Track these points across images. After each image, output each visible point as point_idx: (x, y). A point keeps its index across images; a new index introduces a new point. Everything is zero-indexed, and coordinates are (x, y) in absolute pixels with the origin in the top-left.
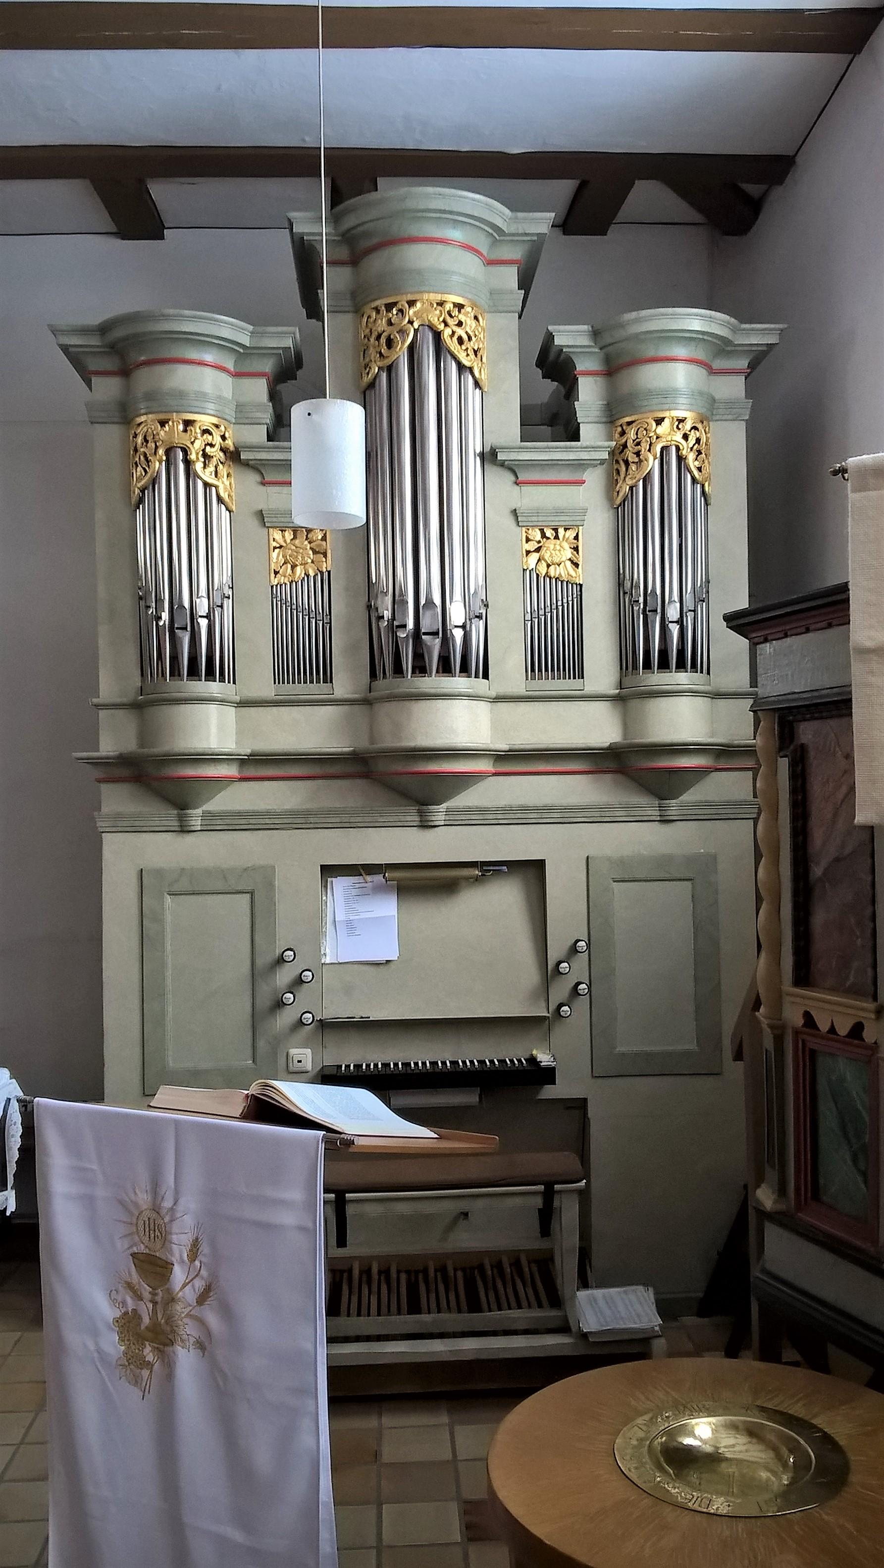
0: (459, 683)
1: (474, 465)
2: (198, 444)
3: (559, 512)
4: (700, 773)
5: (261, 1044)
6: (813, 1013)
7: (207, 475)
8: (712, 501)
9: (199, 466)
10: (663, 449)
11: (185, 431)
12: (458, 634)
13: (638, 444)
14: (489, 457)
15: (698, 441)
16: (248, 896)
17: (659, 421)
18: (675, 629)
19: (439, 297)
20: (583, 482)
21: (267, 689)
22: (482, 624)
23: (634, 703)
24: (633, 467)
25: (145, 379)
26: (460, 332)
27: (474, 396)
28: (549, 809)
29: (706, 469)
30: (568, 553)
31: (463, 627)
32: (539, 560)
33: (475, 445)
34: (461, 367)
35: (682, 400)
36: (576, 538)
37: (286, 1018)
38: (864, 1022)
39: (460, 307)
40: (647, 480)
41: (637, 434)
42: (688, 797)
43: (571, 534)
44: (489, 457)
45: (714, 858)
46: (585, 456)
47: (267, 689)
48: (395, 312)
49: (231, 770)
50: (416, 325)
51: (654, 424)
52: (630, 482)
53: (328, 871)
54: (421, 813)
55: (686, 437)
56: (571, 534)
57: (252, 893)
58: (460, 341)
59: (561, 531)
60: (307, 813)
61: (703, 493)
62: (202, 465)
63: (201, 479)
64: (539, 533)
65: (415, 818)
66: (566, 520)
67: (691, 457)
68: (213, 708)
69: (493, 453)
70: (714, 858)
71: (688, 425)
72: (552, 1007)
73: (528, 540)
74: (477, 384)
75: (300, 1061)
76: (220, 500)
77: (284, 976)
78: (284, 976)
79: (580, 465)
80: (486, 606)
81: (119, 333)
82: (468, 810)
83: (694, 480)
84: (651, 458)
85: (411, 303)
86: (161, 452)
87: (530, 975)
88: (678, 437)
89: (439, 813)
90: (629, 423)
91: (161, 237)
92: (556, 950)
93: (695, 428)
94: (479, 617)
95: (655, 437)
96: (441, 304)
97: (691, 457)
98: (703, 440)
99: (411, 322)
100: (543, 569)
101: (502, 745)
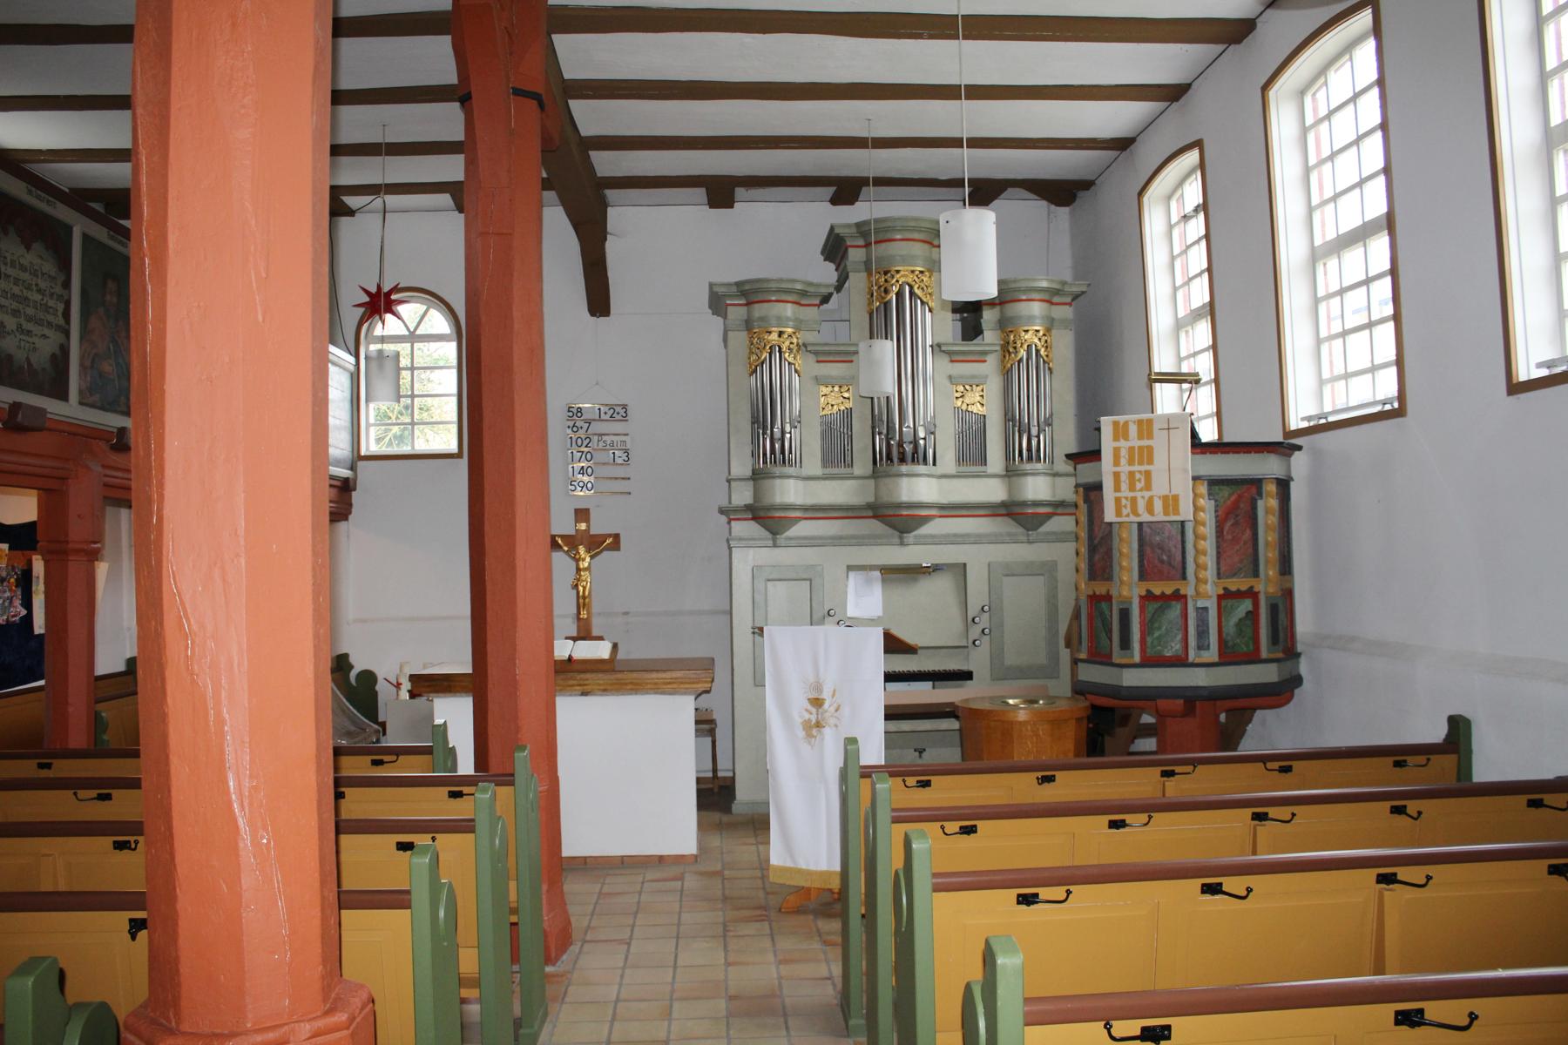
0: (921, 469)
1: (929, 350)
2: (787, 343)
3: (973, 377)
4: (1049, 516)
7: (791, 360)
8: (1054, 371)
10: (1028, 346)
12: (922, 442)
14: (937, 348)
15: (1046, 341)
16: (808, 582)
17: (1027, 331)
19: (912, 268)
20: (985, 361)
21: (819, 471)
22: (933, 436)
23: (1014, 479)
24: (1013, 355)
25: (759, 310)
26: (922, 285)
27: (928, 315)
28: (968, 535)
29: (1050, 356)
30: (979, 399)
31: (925, 439)
33: (929, 342)
34: (922, 302)
35: (1038, 321)
36: (983, 390)
39: (921, 272)
42: (1043, 529)
44: (937, 348)
46: (987, 348)
47: (819, 471)
48: (889, 275)
49: (798, 514)
50: (900, 283)
52: (1011, 362)
53: (850, 568)
54: (901, 538)
55: (1040, 339)
56: (979, 388)
57: (811, 580)
59: (974, 386)
60: (841, 538)
61: (1049, 369)
65: (897, 540)
66: (977, 381)
68: (792, 481)
69: (939, 345)
71: (1041, 333)
72: (971, 641)
74: (930, 310)
76: (796, 371)
79: (985, 353)
80: (935, 426)
81: (747, 287)
82: (925, 536)
83: (1044, 360)
85: (898, 272)
87: (958, 625)
88: (1036, 340)
89: (910, 537)
90: (1012, 331)
91: (732, 207)
92: (973, 610)
93: (1044, 335)
94: (932, 433)
96: (913, 272)
97: (1043, 350)
98: (1049, 341)
99: (897, 281)
100: (965, 405)
101: (944, 501)
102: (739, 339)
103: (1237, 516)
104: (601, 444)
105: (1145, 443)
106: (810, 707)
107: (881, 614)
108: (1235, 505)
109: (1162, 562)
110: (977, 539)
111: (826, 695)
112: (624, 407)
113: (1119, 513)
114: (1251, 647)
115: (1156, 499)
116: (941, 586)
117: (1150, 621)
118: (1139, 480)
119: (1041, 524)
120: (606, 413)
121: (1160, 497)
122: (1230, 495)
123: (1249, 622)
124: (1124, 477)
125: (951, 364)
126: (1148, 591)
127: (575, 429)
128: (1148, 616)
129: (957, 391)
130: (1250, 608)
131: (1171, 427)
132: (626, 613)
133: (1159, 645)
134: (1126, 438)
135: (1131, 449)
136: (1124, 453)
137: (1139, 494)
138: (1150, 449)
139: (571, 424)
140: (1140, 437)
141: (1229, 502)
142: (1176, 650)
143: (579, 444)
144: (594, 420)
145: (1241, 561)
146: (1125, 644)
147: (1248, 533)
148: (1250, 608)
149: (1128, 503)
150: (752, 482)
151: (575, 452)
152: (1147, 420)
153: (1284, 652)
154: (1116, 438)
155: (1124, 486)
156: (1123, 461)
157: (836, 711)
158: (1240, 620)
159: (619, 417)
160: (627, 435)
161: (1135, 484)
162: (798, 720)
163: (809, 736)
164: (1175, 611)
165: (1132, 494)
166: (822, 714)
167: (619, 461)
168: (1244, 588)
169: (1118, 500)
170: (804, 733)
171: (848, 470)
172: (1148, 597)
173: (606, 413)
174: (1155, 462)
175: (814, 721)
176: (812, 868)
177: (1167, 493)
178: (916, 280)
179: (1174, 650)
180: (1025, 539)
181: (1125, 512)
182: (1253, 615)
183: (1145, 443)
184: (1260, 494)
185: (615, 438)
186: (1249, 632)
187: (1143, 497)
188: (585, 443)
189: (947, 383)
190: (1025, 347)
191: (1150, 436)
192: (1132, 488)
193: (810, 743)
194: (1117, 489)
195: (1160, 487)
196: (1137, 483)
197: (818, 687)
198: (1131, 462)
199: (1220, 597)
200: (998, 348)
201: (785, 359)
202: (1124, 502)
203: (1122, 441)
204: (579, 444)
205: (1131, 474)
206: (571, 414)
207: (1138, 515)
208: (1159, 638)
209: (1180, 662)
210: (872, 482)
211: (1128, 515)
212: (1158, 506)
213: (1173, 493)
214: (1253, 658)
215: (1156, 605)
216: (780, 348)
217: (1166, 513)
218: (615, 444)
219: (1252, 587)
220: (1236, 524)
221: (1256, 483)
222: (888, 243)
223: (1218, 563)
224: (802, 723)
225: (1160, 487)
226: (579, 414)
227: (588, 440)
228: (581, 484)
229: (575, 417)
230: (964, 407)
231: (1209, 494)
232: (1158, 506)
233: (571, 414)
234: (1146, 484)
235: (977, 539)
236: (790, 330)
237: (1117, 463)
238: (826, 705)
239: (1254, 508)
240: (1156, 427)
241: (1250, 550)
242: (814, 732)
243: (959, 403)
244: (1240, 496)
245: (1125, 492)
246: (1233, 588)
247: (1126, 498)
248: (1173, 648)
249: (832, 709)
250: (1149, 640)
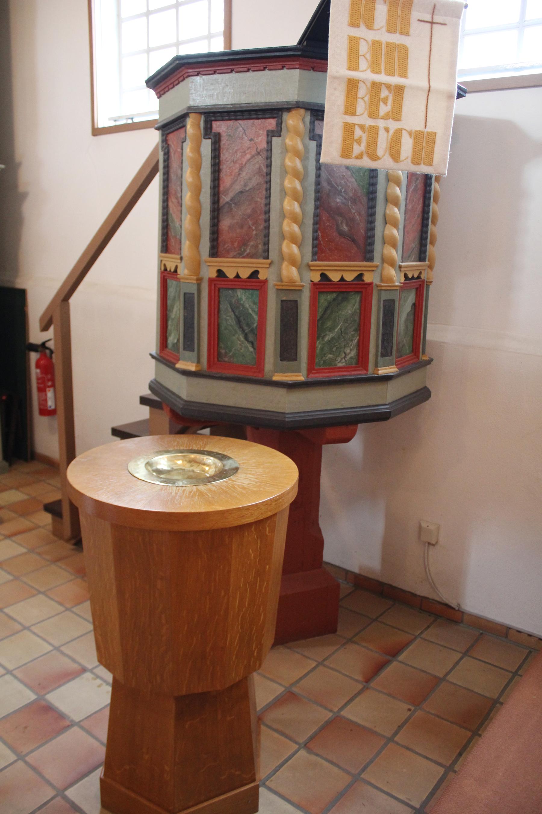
6: (224, 270)
38: (259, 269)
105: (396, 39)
109: (341, 234)
113: (346, 152)
115: (405, 135)
118: (385, 102)
121: (410, 134)
128: (320, 311)
131: (435, 21)
136: (364, 48)
137: (381, 124)
138: (404, 51)
142: (351, 358)
154: (354, 24)
155: (361, 107)
156: (363, 64)
161: (378, 107)
165: (369, 122)
169: (348, 129)
174: (410, 74)
177: (421, 128)
179: (348, 357)
181: (357, 149)
183: (396, 39)
187: (387, 130)
191: (405, 32)
194: (350, 110)
202: (358, 132)
203: (362, 26)
205: (376, 87)
208: (329, 341)
211: (359, 157)
213: (429, 129)
237: (353, 65)
247: (362, 127)
250: (319, 345)
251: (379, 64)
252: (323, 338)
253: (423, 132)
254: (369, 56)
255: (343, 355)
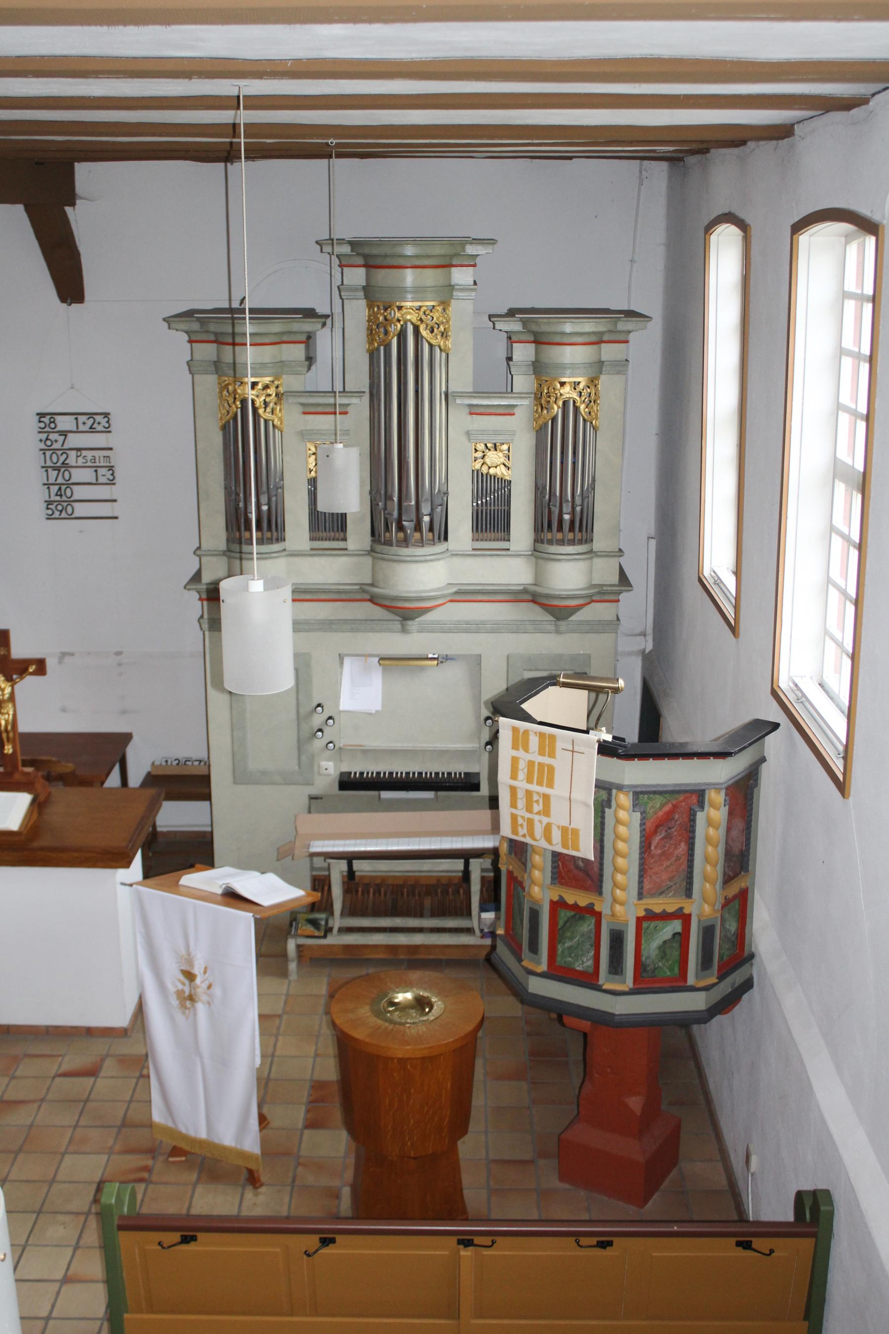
3: (496, 433)
4: (579, 608)
5: (303, 757)
9: (261, 411)
11: (253, 388)
13: (549, 397)
17: (563, 384)
18: (567, 517)
20: (513, 414)
24: (545, 412)
28: (483, 623)
30: (502, 460)
31: (429, 515)
32: (483, 464)
37: (319, 743)
40: (554, 420)
41: (548, 389)
42: (574, 618)
43: (505, 447)
45: (589, 657)
51: (558, 386)
54: (403, 625)
56: (505, 447)
58: (432, 331)
62: (263, 410)
63: (262, 417)
64: (483, 446)
67: (582, 407)
70: (589, 657)
73: (476, 450)
75: (326, 769)
77: (318, 719)
78: (318, 719)
82: (432, 622)
83: (584, 420)
84: (555, 407)
86: (238, 403)
88: (575, 395)
89: (413, 625)
95: (559, 394)
98: (593, 395)
102: (209, 382)
103: (670, 828)
104: (81, 460)
105: (546, 760)
106: (182, 978)
107: (379, 708)
108: (669, 816)
110: (496, 628)
111: (197, 970)
112: (106, 415)
114: (676, 970)
116: (454, 673)
117: (562, 927)
119: (571, 614)
120: (84, 423)
121: (558, 827)
122: (662, 806)
123: (676, 945)
124: (520, 794)
125: (469, 417)
126: (561, 897)
127: (49, 443)
129: (476, 450)
130: (679, 929)
132: (119, 653)
133: (570, 956)
134: (526, 749)
135: (531, 764)
136: (522, 765)
137: (536, 818)
138: (551, 769)
139: (44, 436)
140: (541, 752)
141: (661, 813)
142: (588, 966)
143: (55, 460)
144: (71, 432)
145: (671, 879)
146: (534, 947)
147: (683, 847)
148: (679, 929)
149: (525, 824)
150: (225, 559)
151: (50, 470)
152: (549, 735)
153: (717, 978)
154: (515, 747)
155: (521, 803)
156: (521, 775)
157: (209, 987)
158: (665, 942)
159: (99, 428)
160: (111, 449)
161: (532, 806)
162: (172, 989)
163: (183, 1006)
164: (587, 926)
165: (528, 815)
166: (194, 989)
167: (102, 480)
168: (671, 909)
169: (514, 818)
170: (178, 1002)
171: (341, 544)
172: (557, 905)
173: (84, 423)
174: (555, 786)
175: (187, 993)
176: (192, 1133)
177: (566, 824)
178: (423, 317)
179: (585, 965)
180: (551, 628)
182: (683, 937)
183: (546, 760)
184: (702, 807)
185: (97, 453)
186: (676, 954)
187: (540, 821)
188: (62, 458)
189: (464, 439)
190: (560, 403)
191: (552, 755)
192: (529, 809)
193: (184, 1013)
194: (514, 805)
195: (559, 816)
196: (535, 805)
197: (190, 961)
198: (529, 780)
199: (639, 920)
200: (533, 396)
201: (259, 416)
202: (520, 821)
204: (55, 460)
206: (42, 425)
207: (535, 840)
208: (570, 948)
209: (589, 980)
210: (368, 560)
211: (524, 836)
212: (556, 835)
213: (572, 826)
214: (678, 984)
215: (570, 913)
216: (253, 401)
217: (565, 845)
218: (97, 460)
219: (681, 909)
220: (668, 837)
221: (699, 795)
222: (387, 270)
223: (641, 883)
224: (175, 992)
225: (559, 816)
226: (52, 425)
227: (64, 456)
228: (60, 508)
229: (47, 429)
230: (485, 470)
231: (634, 806)
232: (556, 835)
233: (42, 425)
234: (544, 804)
235: (496, 628)
236: (267, 380)
237: (514, 776)
238: (198, 981)
239: (692, 820)
240: (559, 745)
241: (684, 866)
242: (188, 1003)
243: (477, 466)
244: (675, 807)
245: (521, 812)
246: (658, 910)
247: (523, 817)
248: (584, 964)
249: (204, 986)
250: (560, 948)
251: (533, 778)
252: (564, 943)
253: (567, 828)
254: (526, 770)
255: (581, 962)
